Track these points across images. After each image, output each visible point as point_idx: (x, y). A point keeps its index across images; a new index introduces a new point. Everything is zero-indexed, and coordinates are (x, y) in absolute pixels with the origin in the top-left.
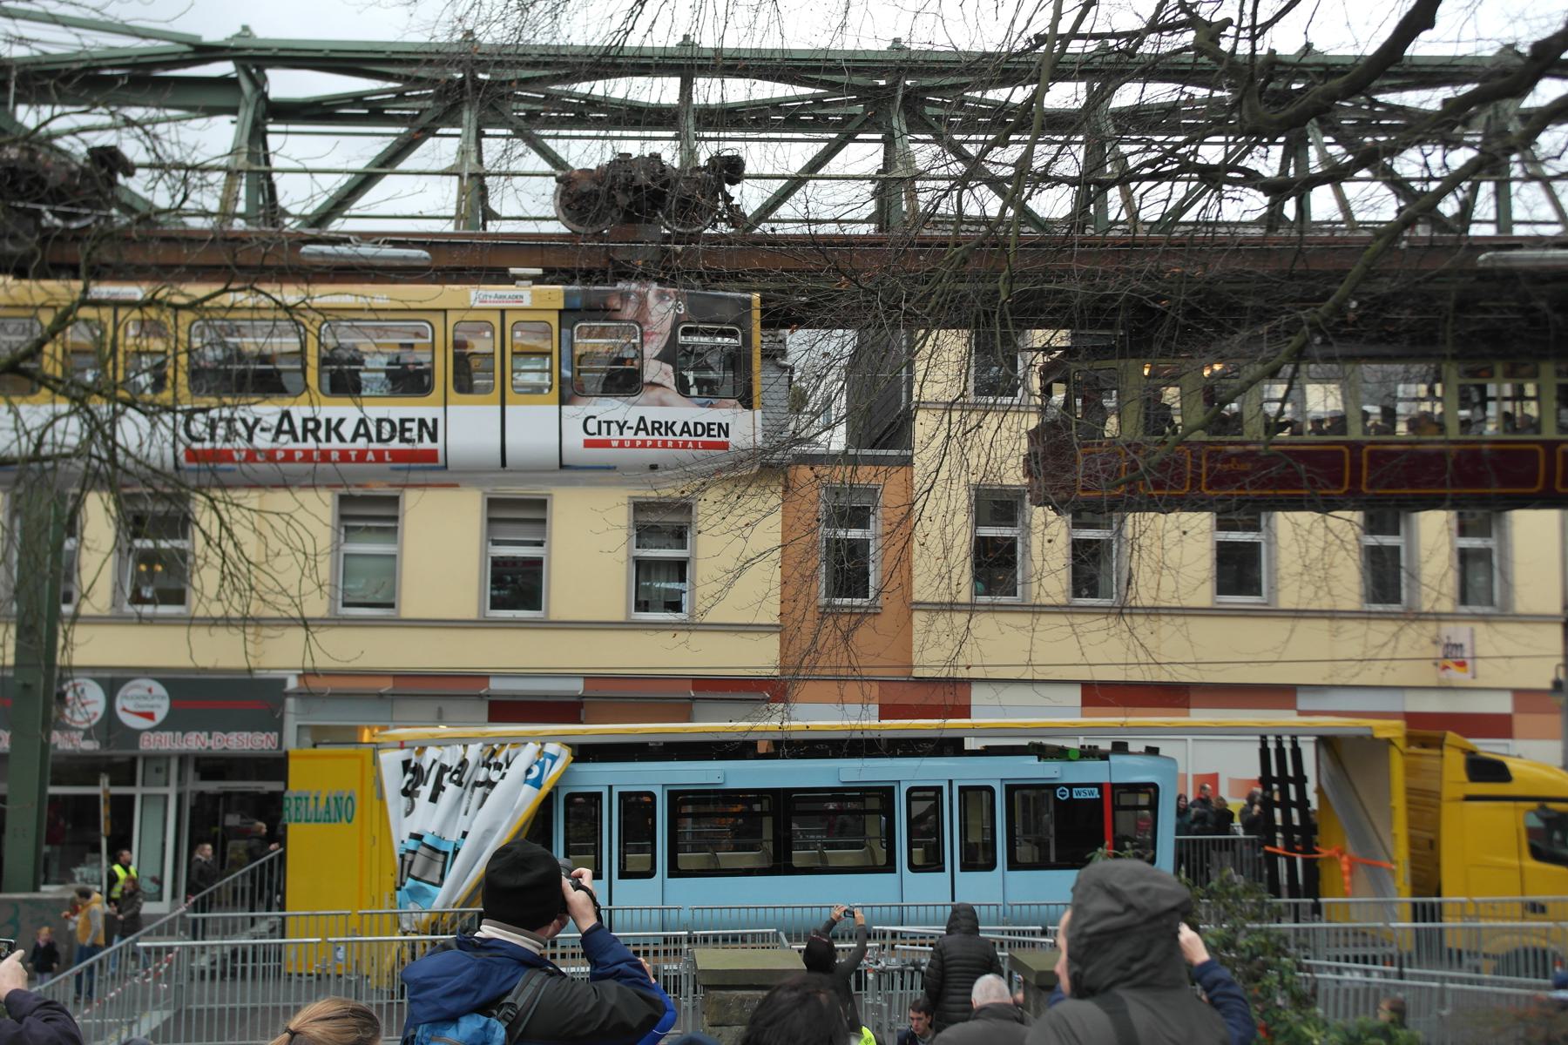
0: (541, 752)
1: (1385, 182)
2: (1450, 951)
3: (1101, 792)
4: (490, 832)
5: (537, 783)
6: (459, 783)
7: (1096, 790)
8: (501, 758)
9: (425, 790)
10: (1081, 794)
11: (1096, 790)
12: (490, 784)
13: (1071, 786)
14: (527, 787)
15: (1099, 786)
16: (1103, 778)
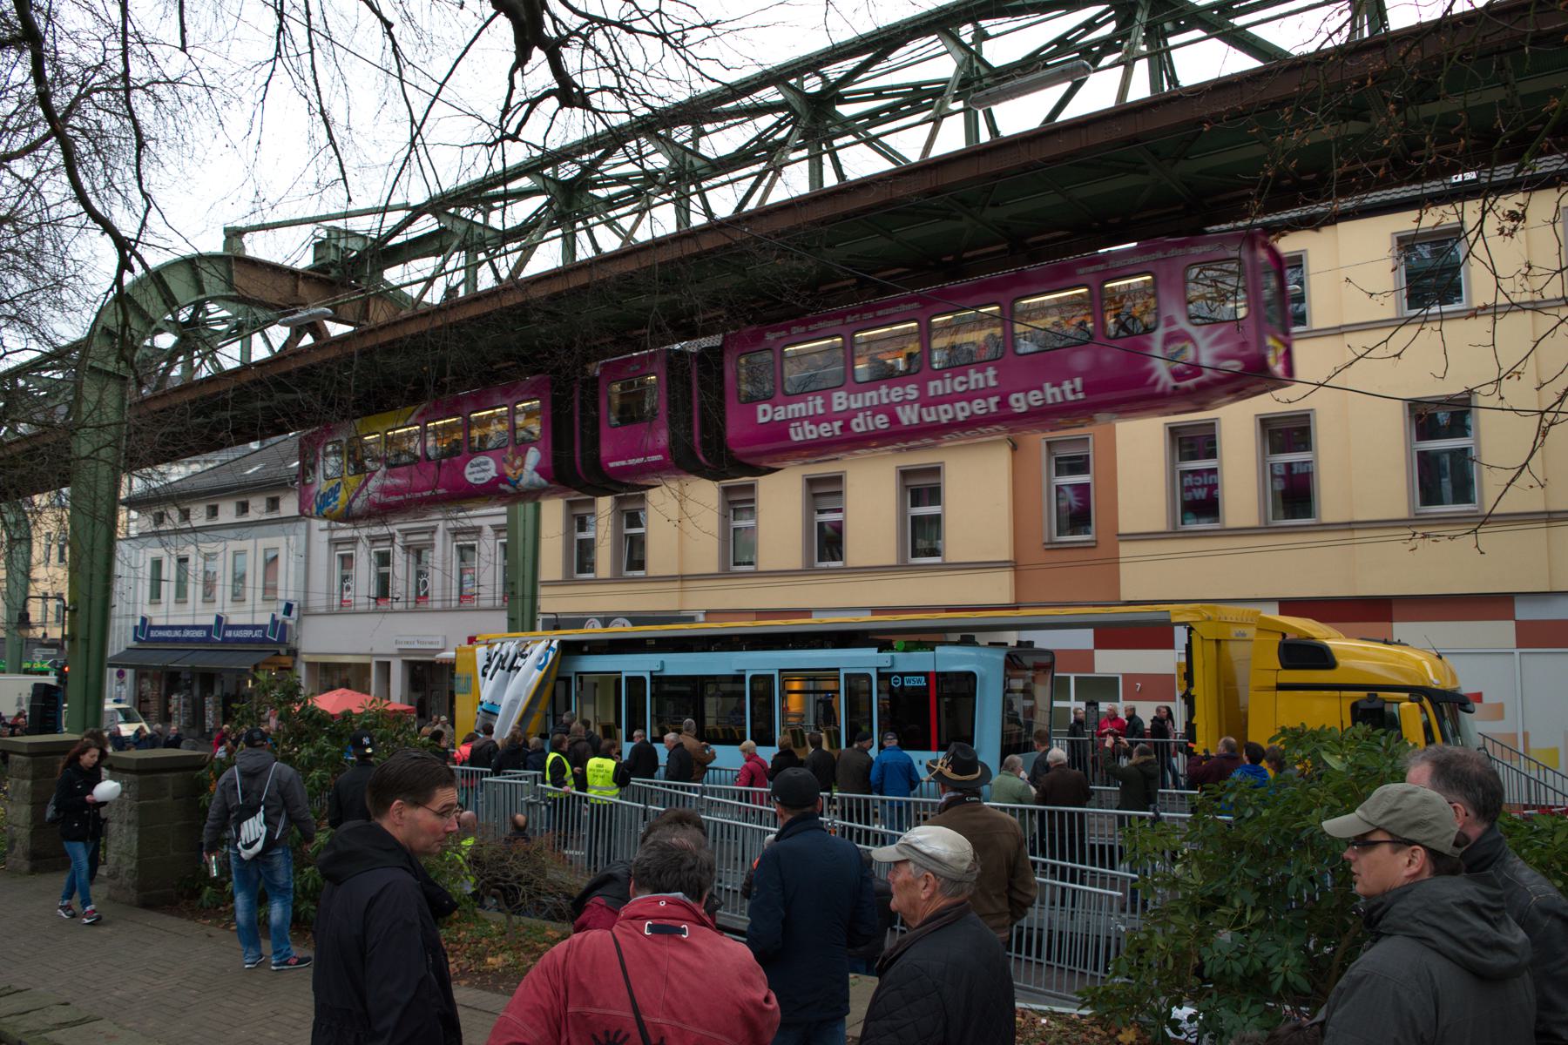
0: (549, 647)
1: (1219, 37)
2: (1092, 846)
3: (926, 681)
4: (514, 702)
5: (540, 668)
6: (503, 668)
7: (923, 678)
8: (527, 651)
9: (489, 673)
10: (910, 682)
11: (923, 678)
12: (518, 669)
13: (902, 675)
14: (537, 671)
15: (925, 674)
16: (929, 668)
